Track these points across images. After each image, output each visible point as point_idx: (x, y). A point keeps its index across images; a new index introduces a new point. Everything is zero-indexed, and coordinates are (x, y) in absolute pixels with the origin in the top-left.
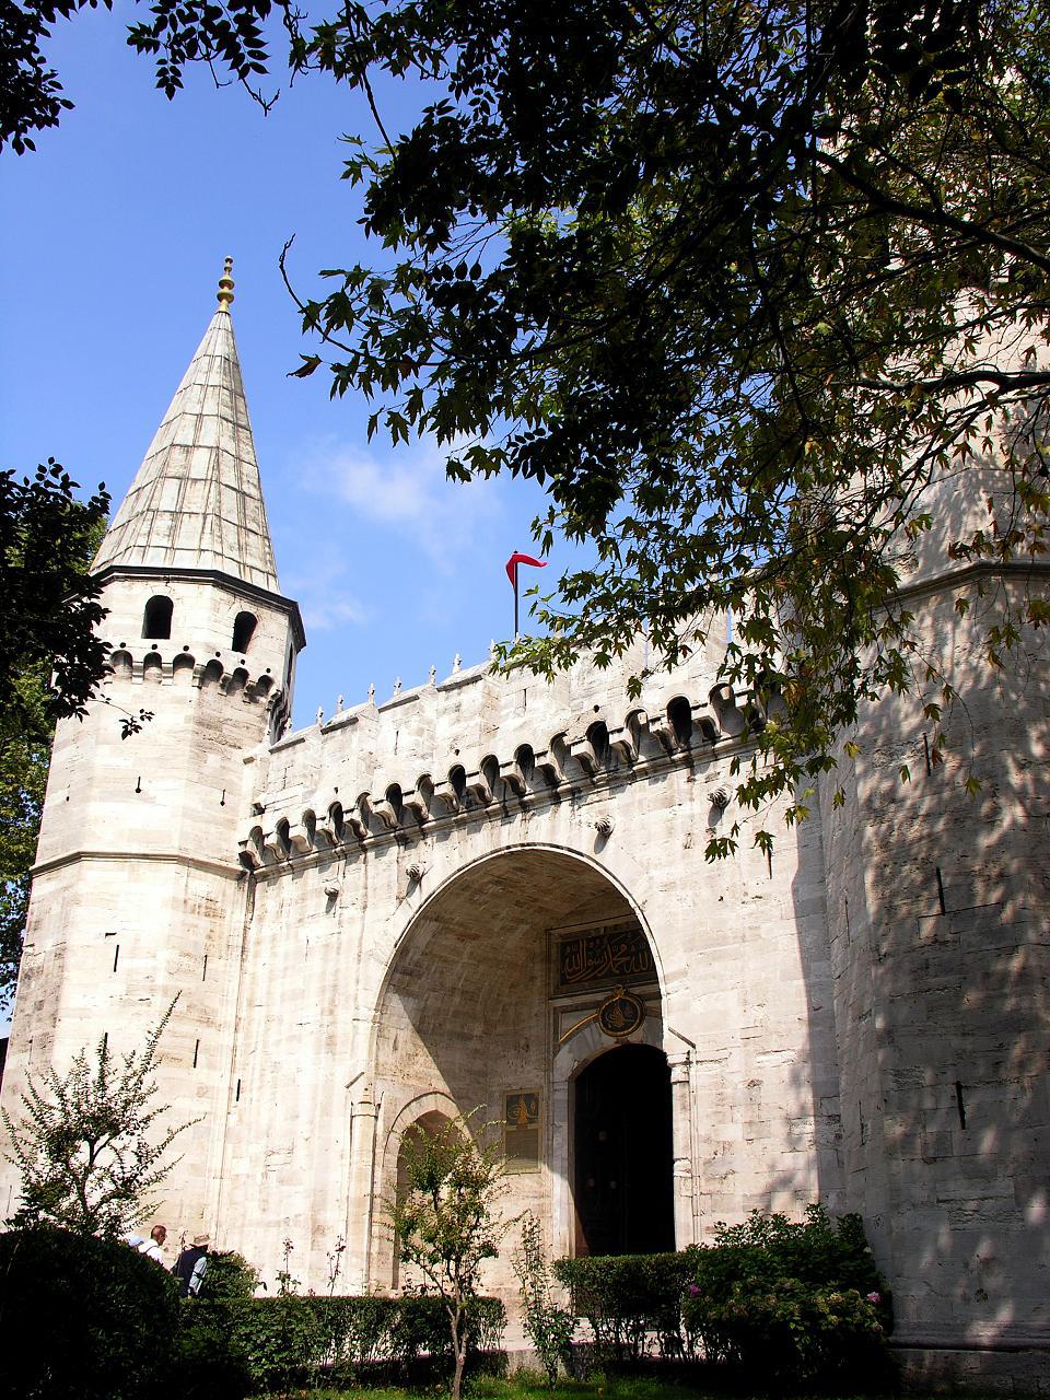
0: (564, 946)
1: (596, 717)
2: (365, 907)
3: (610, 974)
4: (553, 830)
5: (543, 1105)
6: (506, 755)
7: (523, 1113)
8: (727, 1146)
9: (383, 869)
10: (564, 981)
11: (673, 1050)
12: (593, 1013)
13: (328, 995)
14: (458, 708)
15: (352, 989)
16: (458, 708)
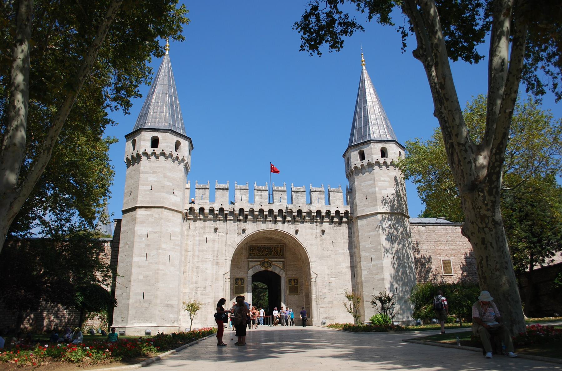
0: (250, 247)
1: (299, 208)
2: (227, 234)
3: (263, 255)
4: (283, 228)
5: (245, 281)
6: (276, 210)
7: (240, 283)
8: (325, 293)
9: (232, 226)
10: (250, 255)
11: (313, 275)
12: (259, 263)
13: (216, 253)
14: (261, 195)
15: (224, 252)
16: (261, 195)
